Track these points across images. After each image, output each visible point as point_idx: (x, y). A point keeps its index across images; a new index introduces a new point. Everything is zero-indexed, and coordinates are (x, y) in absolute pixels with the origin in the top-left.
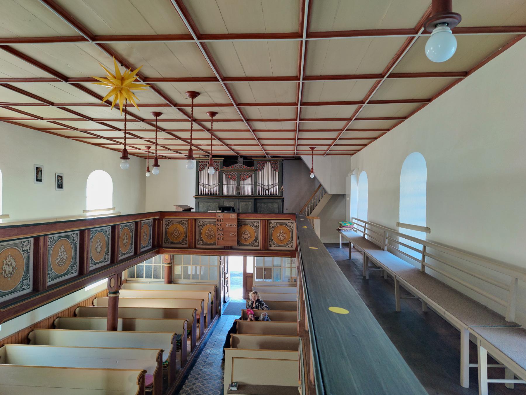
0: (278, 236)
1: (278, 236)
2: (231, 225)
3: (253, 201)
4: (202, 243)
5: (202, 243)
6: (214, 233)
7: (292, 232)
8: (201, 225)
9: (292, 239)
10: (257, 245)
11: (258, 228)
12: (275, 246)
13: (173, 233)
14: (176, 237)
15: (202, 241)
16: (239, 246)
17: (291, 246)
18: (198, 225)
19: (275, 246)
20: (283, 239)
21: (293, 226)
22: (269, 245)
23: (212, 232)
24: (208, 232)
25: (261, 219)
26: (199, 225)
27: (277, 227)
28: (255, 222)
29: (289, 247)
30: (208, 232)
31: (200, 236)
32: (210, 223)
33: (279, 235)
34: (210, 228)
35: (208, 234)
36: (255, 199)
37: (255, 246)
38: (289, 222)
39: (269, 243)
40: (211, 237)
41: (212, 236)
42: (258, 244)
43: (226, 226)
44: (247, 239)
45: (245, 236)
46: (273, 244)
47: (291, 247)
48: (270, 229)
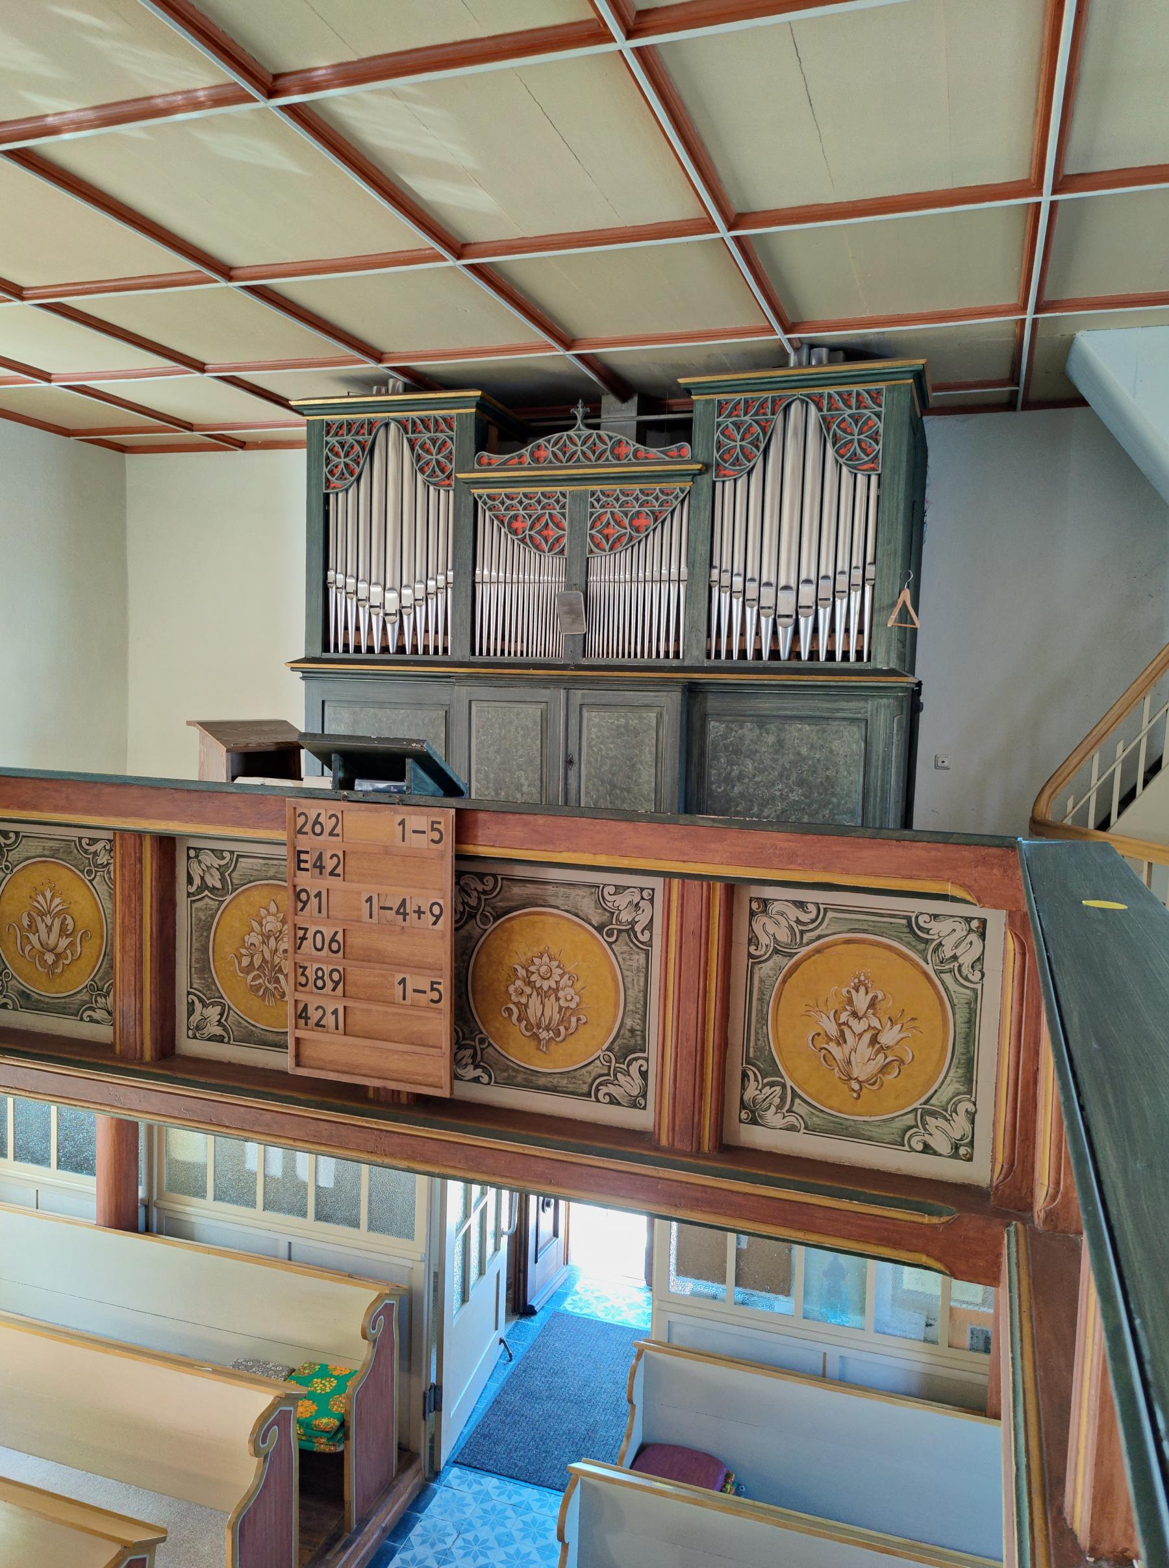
1: (829, 1039)
2: (402, 910)
3: (671, 701)
8: (210, 882)
9: (969, 1079)
10: (635, 1092)
11: (650, 943)
12: (791, 1119)
13: (33, 927)
14: (50, 958)
16: (485, 1079)
17: (956, 1147)
18: (190, 880)
19: (791, 1119)
21: (980, 959)
22: (743, 1105)
24: (254, 939)
25: (668, 875)
26: (197, 881)
27: (818, 951)
28: (619, 889)
29: (927, 1149)
30: (254, 939)
31: (203, 967)
32: (271, 874)
33: (833, 1030)
34: (273, 908)
35: (257, 961)
36: (692, 691)
37: (614, 1101)
38: (935, 917)
39: (743, 1088)
40: (277, 981)
42: (638, 1080)
43: (366, 918)
44: (548, 1029)
45: (534, 1003)
46: (779, 1107)
47: (955, 1155)
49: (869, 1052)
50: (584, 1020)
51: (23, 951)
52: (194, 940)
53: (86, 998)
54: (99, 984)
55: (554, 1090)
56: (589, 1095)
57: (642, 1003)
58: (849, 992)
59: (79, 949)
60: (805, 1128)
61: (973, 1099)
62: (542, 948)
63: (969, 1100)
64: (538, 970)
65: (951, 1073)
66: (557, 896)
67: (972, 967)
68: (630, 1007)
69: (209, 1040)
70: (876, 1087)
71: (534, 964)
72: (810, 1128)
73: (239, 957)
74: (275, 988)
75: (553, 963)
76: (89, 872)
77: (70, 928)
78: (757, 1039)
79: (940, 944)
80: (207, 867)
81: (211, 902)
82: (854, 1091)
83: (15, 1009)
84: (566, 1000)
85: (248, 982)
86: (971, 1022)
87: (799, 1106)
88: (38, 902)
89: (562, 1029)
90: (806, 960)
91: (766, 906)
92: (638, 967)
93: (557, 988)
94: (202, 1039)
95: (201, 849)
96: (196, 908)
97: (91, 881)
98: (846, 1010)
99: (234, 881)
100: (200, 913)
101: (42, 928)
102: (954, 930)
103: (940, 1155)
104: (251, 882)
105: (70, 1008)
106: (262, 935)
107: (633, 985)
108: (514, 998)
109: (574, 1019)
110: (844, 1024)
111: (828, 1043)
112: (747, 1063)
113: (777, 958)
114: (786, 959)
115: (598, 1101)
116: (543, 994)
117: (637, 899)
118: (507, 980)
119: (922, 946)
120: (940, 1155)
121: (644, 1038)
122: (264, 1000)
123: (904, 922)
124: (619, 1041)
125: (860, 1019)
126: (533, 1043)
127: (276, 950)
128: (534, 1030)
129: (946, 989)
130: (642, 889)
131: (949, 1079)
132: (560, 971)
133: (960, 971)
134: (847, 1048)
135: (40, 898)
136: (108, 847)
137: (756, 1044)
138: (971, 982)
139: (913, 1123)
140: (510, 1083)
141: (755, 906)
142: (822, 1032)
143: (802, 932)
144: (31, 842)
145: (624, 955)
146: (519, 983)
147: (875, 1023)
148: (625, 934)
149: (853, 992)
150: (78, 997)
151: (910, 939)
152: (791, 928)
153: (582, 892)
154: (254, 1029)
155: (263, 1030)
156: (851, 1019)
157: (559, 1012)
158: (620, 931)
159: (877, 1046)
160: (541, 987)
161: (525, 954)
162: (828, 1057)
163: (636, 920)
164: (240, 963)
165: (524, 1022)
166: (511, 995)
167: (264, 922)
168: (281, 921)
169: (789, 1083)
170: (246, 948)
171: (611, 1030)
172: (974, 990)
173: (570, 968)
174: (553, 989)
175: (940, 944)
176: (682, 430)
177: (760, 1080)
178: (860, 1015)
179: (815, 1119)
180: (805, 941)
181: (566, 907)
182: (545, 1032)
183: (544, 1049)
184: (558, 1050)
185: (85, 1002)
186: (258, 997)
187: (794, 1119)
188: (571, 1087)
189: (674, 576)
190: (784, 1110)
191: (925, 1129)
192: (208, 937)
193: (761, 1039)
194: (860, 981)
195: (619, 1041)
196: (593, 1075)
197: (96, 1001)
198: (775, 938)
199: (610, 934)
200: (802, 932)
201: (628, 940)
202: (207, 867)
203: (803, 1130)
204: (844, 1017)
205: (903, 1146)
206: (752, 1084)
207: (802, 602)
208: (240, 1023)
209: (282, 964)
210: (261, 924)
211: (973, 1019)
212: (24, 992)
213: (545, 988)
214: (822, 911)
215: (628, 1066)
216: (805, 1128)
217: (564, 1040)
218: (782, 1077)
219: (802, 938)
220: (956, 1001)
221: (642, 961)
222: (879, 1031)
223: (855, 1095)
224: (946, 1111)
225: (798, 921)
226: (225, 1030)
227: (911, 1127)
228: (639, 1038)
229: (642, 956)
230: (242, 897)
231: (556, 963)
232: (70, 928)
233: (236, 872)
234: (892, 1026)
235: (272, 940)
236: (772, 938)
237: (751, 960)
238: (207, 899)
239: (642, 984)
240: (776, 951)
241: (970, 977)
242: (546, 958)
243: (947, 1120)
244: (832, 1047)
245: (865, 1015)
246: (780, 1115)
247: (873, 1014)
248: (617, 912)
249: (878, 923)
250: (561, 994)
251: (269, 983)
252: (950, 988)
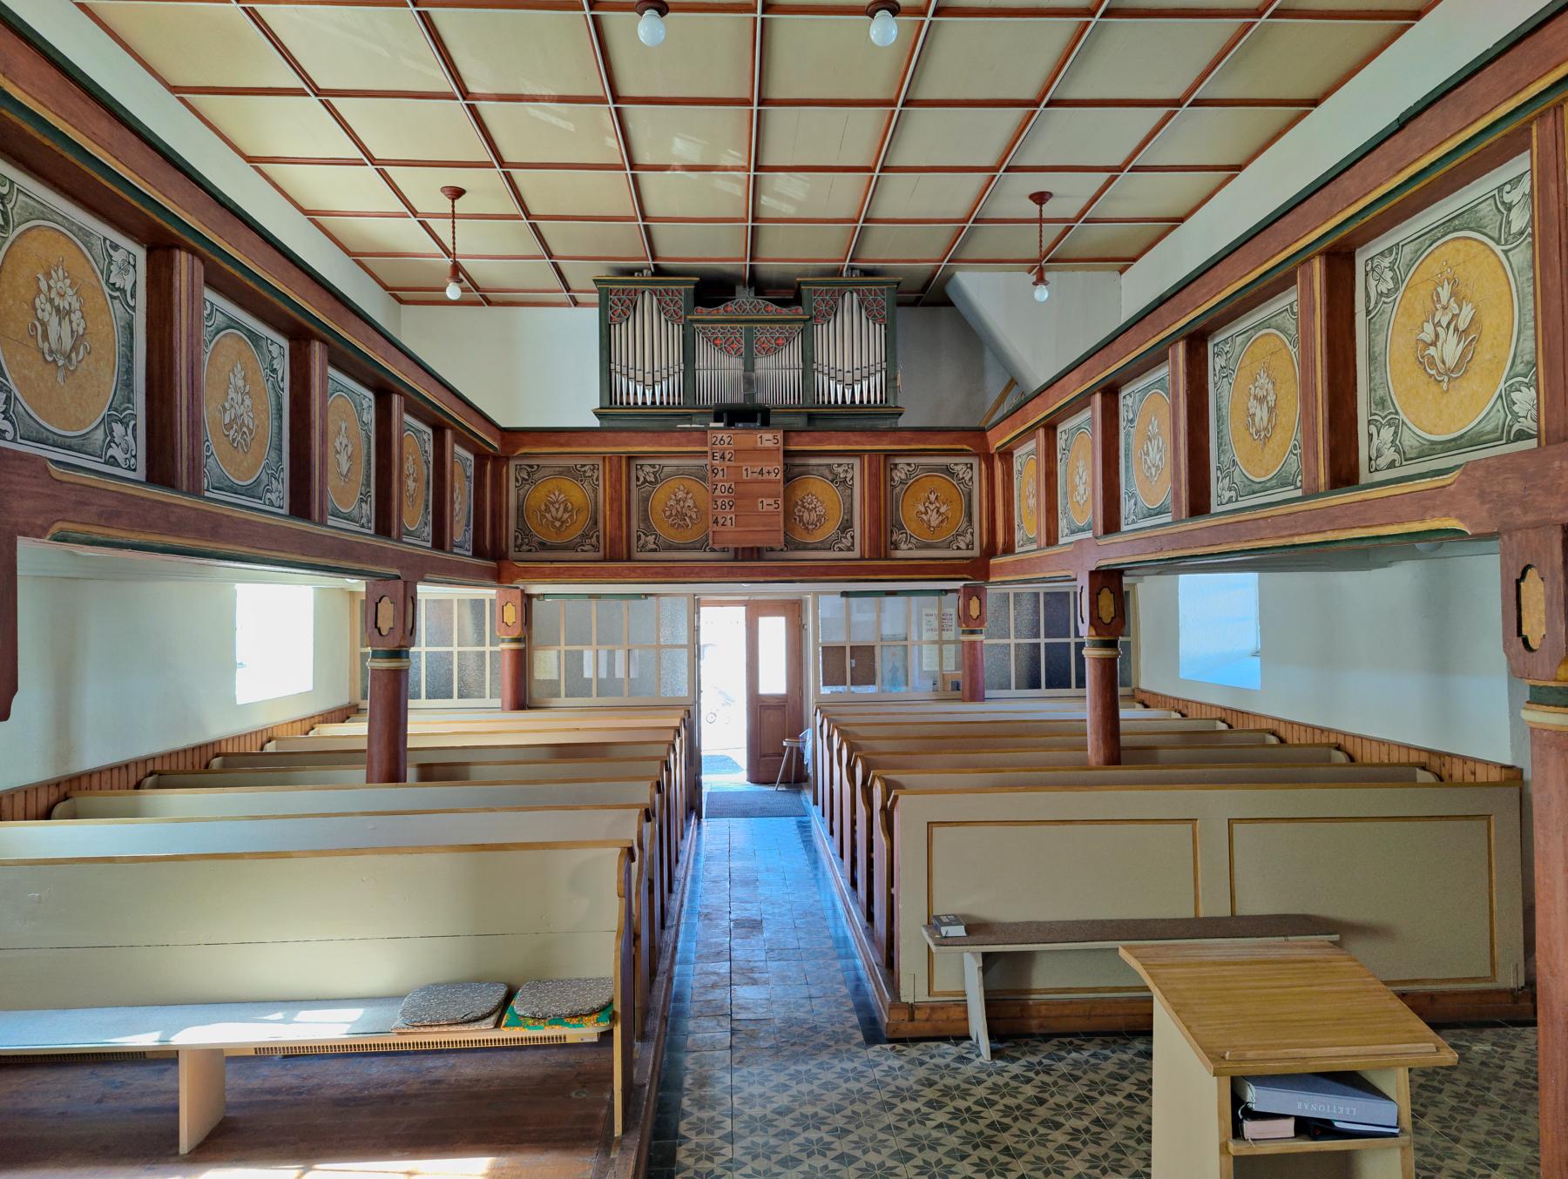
13: (548, 510)
14: (558, 524)
20: (937, 522)
21: (971, 478)
23: (690, 503)
30: (672, 502)
31: (645, 518)
33: (923, 509)
35: (674, 513)
39: (892, 536)
41: (690, 517)
42: (850, 540)
45: (806, 514)
49: (936, 516)
73: (664, 512)
86: (970, 500)
87: (913, 541)
101: (553, 510)
116: (810, 511)
162: (922, 520)
176: (797, 300)
189: (796, 366)
207: (855, 378)
244: (923, 516)
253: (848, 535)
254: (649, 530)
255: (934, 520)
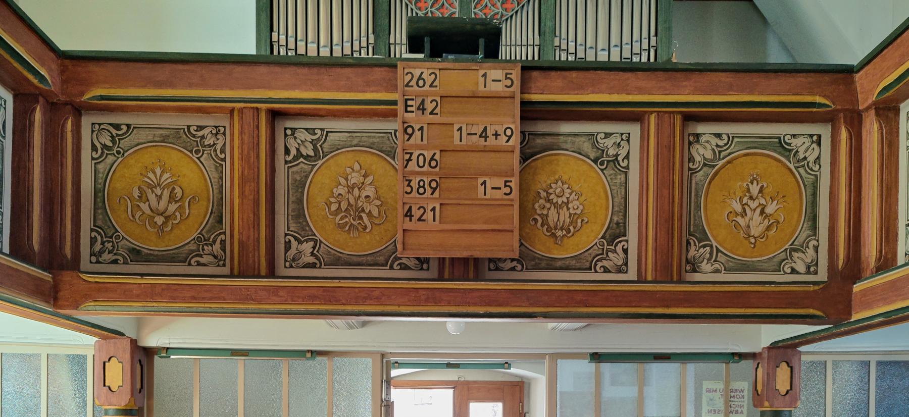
0: (737, 214)
1: (737, 214)
4: (312, 254)
5: (312, 254)
6: (378, 198)
7: (810, 191)
9: (814, 228)
10: (620, 263)
11: (628, 167)
12: (717, 266)
13: (143, 197)
14: (159, 220)
15: (311, 244)
16: (519, 267)
17: (808, 267)
18: (287, 151)
19: (717, 266)
20: (762, 228)
21: (818, 158)
22: (688, 262)
24: (342, 190)
26: (293, 152)
27: (729, 162)
28: (607, 135)
29: (794, 271)
30: (342, 190)
31: (299, 215)
32: (355, 142)
33: (738, 208)
34: (357, 167)
35: (344, 206)
37: (606, 270)
38: (794, 136)
39: (687, 251)
40: (361, 218)
41: (370, 214)
42: (622, 255)
44: (562, 229)
45: (553, 215)
46: (709, 260)
47: (808, 272)
48: (693, 172)
49: (760, 219)
50: (586, 220)
51: (133, 216)
52: (291, 196)
53: (194, 248)
54: (206, 236)
55: (567, 268)
56: (590, 269)
57: (623, 205)
58: (747, 185)
59: (187, 211)
60: (725, 270)
61: (817, 239)
62: (557, 177)
63: (815, 239)
64: (555, 191)
65: (805, 225)
66: (567, 143)
67: (815, 162)
68: (616, 209)
69: (303, 267)
70: (764, 239)
71: (552, 188)
72: (727, 270)
73: (329, 204)
74: (360, 223)
75: (564, 186)
76: (197, 152)
77: (179, 195)
78: (695, 220)
79: (797, 152)
80: (302, 141)
81: (306, 167)
82: (752, 243)
83: (125, 263)
84: (574, 209)
85: (337, 222)
86: (815, 194)
87: (721, 258)
88: (149, 178)
89: (571, 228)
90: (722, 169)
91: (698, 138)
92: (620, 183)
93: (568, 202)
94: (298, 267)
95: (296, 129)
96: (293, 172)
97: (198, 158)
98: (746, 196)
99: (324, 150)
100: (295, 176)
101: (152, 198)
102: (804, 143)
103: (801, 274)
104: (338, 149)
105: (179, 257)
106: (348, 186)
107: (617, 194)
108: (538, 212)
109: (579, 221)
110: (745, 204)
111: (736, 217)
112: (689, 235)
113: (705, 169)
114: (711, 169)
115: (596, 272)
117: (618, 140)
118: (533, 200)
119: (787, 154)
120: (801, 274)
121: (625, 227)
122: (349, 233)
123: (777, 140)
124: (609, 232)
125: (754, 200)
126: (552, 240)
127: (359, 197)
128: (553, 231)
129: (801, 177)
130: (622, 134)
131: (804, 229)
132: (569, 191)
133: (808, 165)
134: (747, 218)
135: (151, 175)
136: (214, 132)
137: (695, 223)
138: (814, 171)
139: (785, 257)
140: (537, 268)
141: (691, 138)
142: (733, 211)
143: (720, 152)
144: (142, 132)
145: (611, 177)
146: (542, 201)
147: (763, 201)
148: (612, 163)
149: (750, 184)
150: (187, 247)
151: (780, 150)
152: (713, 150)
153: (583, 139)
154: (341, 255)
155: (348, 255)
156: (749, 201)
157: (570, 217)
158: (608, 161)
159: (764, 215)
160: (557, 202)
161: (545, 182)
162: (737, 225)
163: (619, 153)
164: (329, 208)
165: (546, 226)
166: (536, 210)
167: (349, 177)
168: (363, 176)
169: (714, 244)
170: (334, 197)
171: (604, 225)
172: (816, 176)
173: (576, 188)
174: (565, 203)
175: (797, 152)
177: (697, 244)
178: (754, 198)
179: (730, 263)
180: (721, 157)
181: (573, 149)
182: (560, 231)
183: (560, 243)
184: (570, 242)
185: (193, 251)
186: (344, 232)
187: (718, 266)
188: (578, 265)
190: (712, 261)
191: (792, 260)
192: (303, 193)
193: (698, 219)
194: (753, 177)
195: (609, 232)
196: (593, 255)
197: (203, 250)
198: (704, 157)
199: (602, 164)
200: (720, 152)
201: (613, 166)
202: (302, 141)
203: (723, 272)
204: (745, 200)
205: (780, 271)
206: (693, 248)
208: (330, 252)
209: (364, 206)
210: (347, 179)
211: (816, 192)
212: (134, 249)
213: (560, 203)
214: (731, 138)
215: (615, 247)
216: (725, 270)
217: (573, 235)
218: (710, 241)
219: (720, 155)
220: (806, 183)
221: (623, 179)
222: (765, 206)
223: (752, 246)
224: (803, 247)
225: (717, 146)
226: (317, 258)
227: (784, 260)
228: (622, 228)
229: (623, 176)
230: (331, 161)
231: (567, 186)
232: (179, 195)
233: (325, 144)
234: (772, 202)
235: (356, 190)
236: (702, 157)
237: (690, 172)
238: (302, 165)
239: (623, 193)
240: (705, 165)
241: (814, 168)
242: (560, 183)
243: (804, 253)
244: (739, 219)
245: (757, 198)
246: (709, 264)
247: (762, 196)
248: (606, 150)
249: (763, 143)
250: (570, 205)
251: (354, 220)
252: (803, 176)
253: (619, 248)
254: (304, 233)
255: (757, 226)
